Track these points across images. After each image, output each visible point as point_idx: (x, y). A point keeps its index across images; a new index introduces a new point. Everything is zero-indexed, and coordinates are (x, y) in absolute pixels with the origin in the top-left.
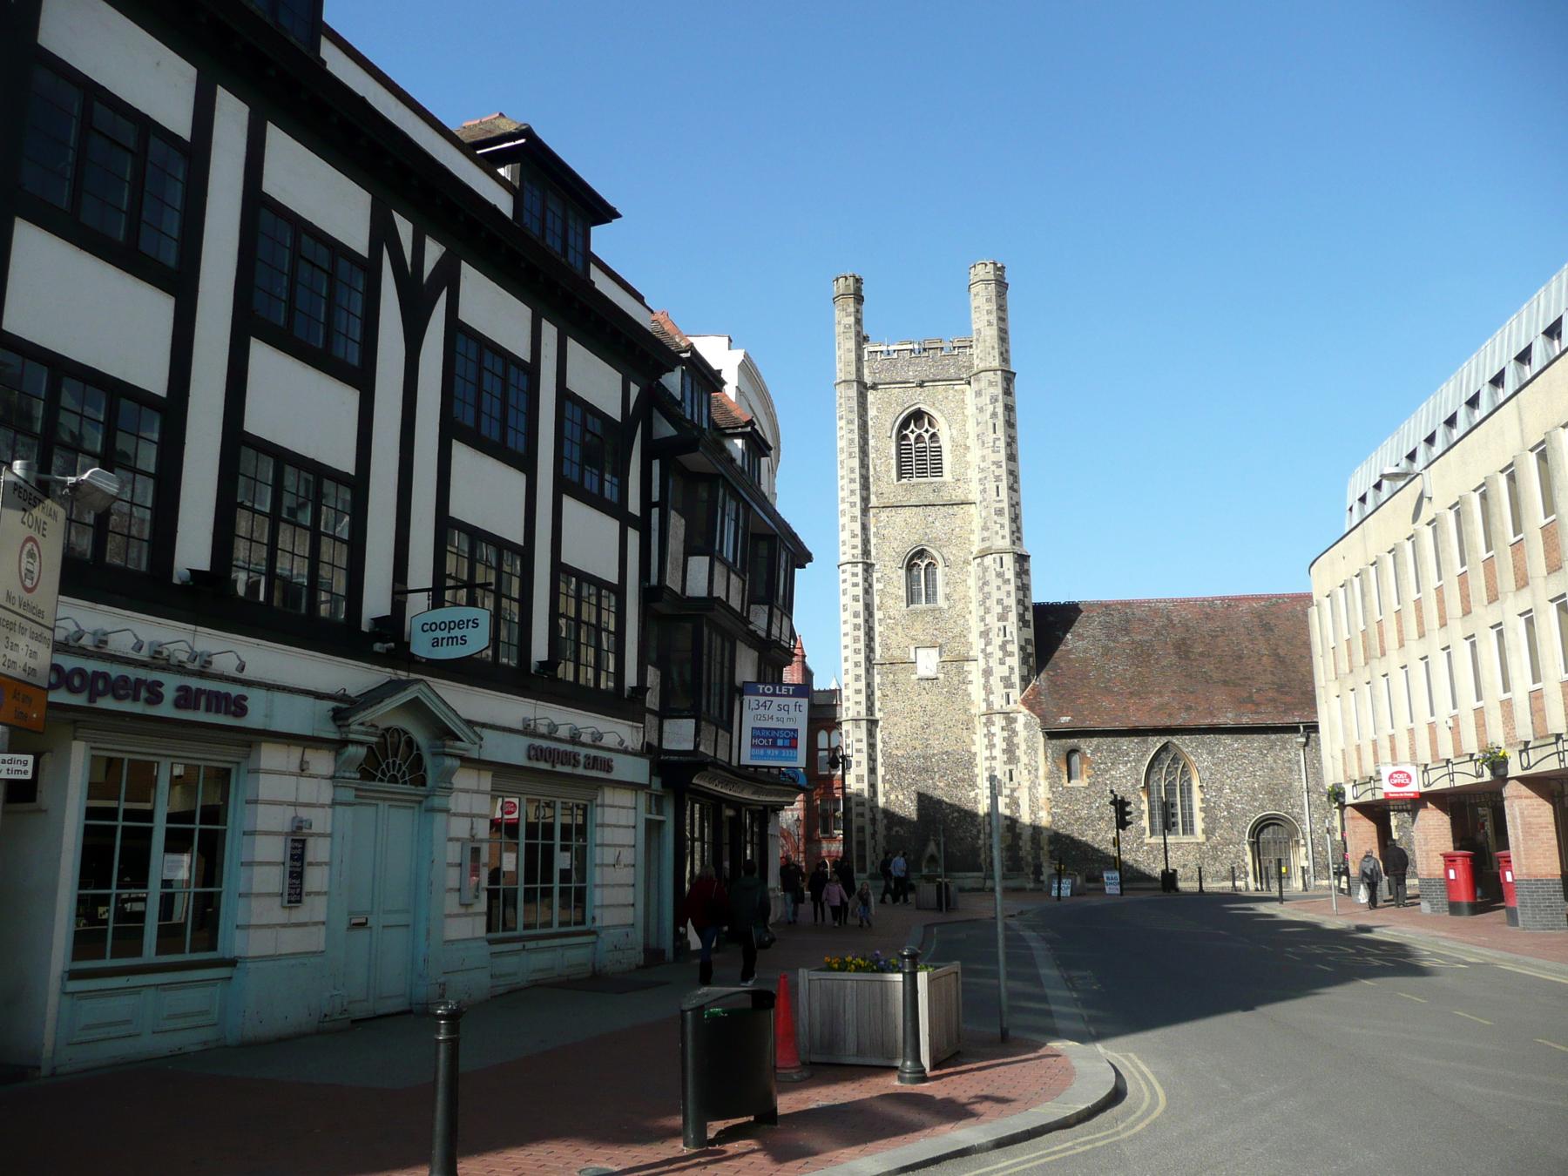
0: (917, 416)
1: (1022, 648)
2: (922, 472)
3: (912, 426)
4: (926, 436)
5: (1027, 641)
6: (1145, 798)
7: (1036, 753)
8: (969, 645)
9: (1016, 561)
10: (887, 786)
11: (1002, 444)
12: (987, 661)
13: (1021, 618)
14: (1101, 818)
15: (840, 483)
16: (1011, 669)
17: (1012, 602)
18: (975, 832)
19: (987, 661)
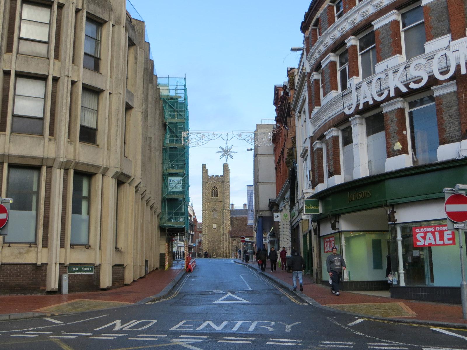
0: (215, 187)
2: (215, 196)
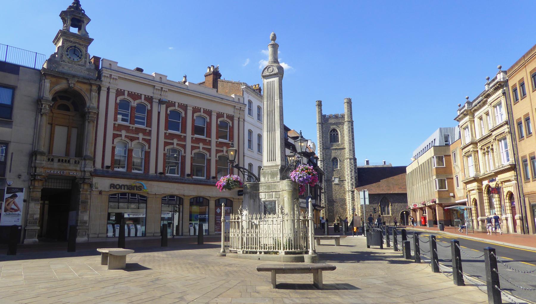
1: (355, 178)
3: (332, 132)
4: (336, 134)
5: (356, 176)
6: (380, 208)
7: (358, 199)
8: (344, 177)
9: (354, 160)
10: (328, 205)
11: (351, 136)
12: (348, 180)
13: (355, 171)
14: (371, 212)
15: (318, 144)
16: (353, 182)
17: (353, 168)
18: (346, 214)
19: (348, 180)
